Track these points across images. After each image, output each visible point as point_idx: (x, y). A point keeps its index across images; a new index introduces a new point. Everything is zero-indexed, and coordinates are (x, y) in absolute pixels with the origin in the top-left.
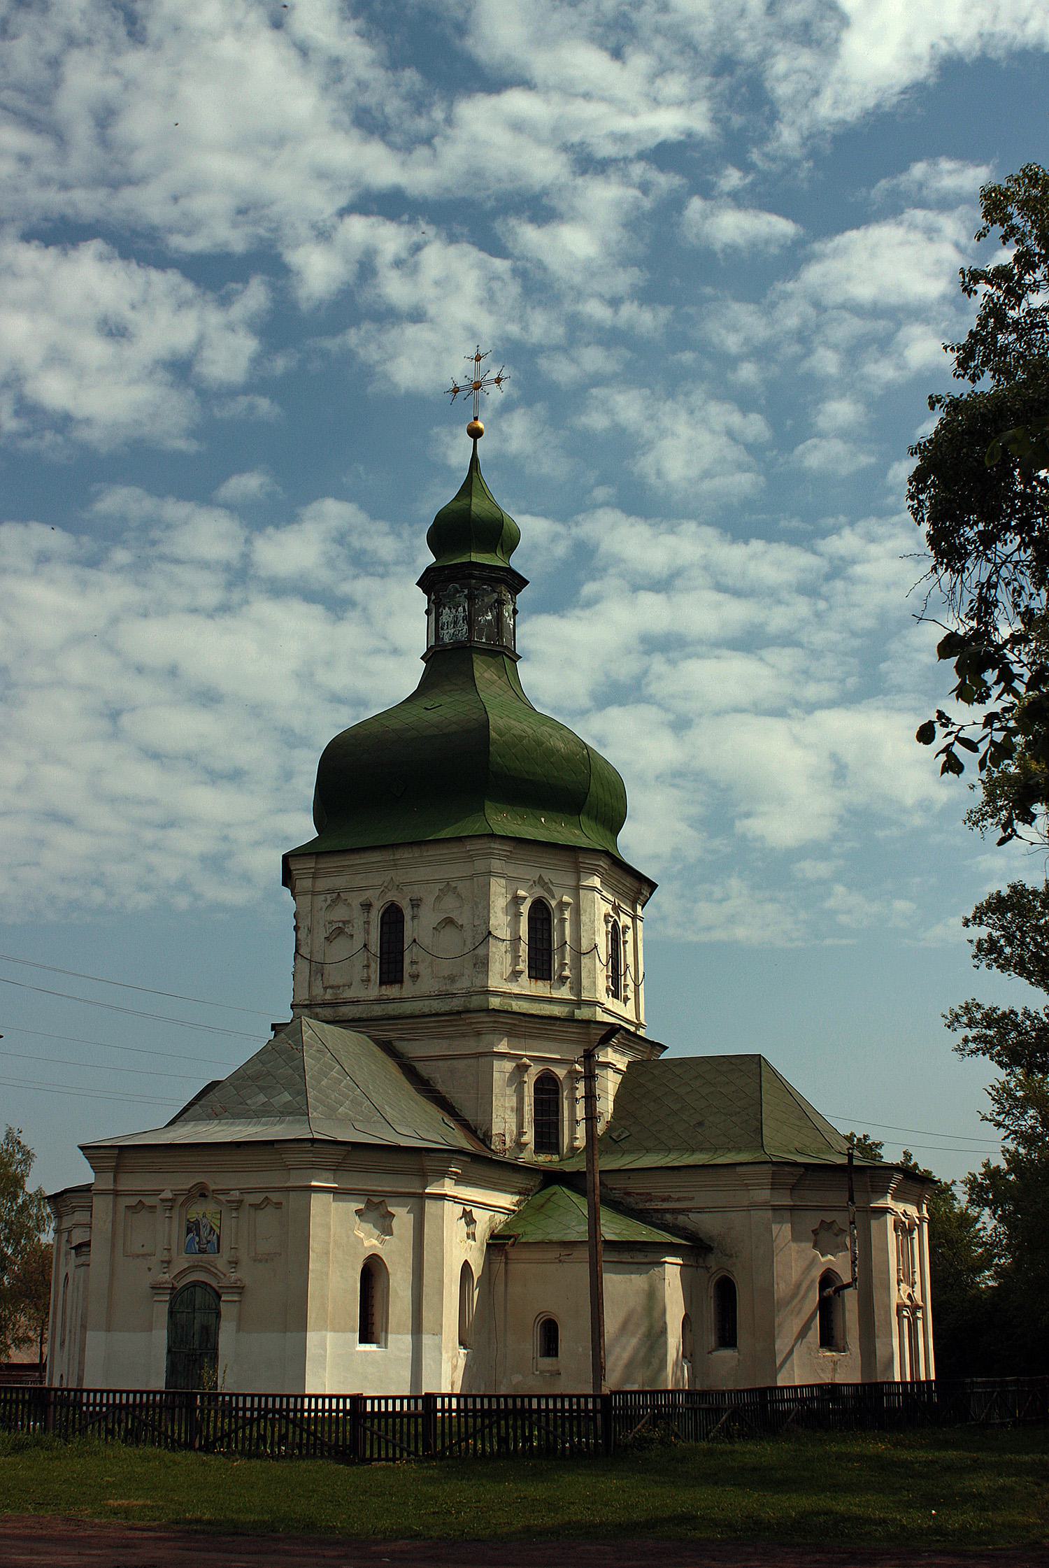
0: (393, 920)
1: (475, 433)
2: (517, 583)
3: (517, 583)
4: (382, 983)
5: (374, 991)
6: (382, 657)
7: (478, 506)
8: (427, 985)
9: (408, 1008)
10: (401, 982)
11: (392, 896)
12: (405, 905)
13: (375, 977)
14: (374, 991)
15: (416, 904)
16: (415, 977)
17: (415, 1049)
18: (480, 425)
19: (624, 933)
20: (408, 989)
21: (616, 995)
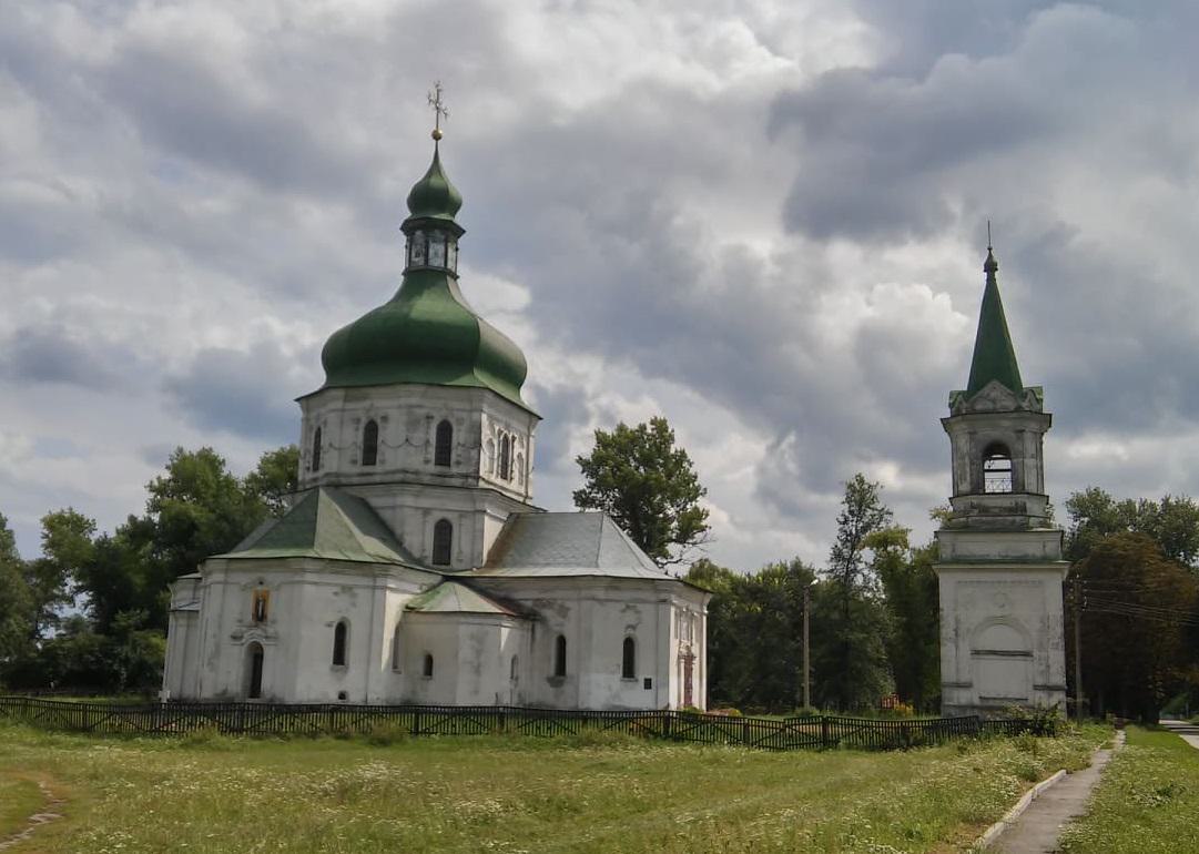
0: (372, 430)
1: (437, 137)
2: (459, 232)
3: (459, 232)
4: (366, 463)
5: (359, 468)
6: (373, 273)
7: (434, 181)
8: (388, 467)
9: (377, 479)
10: (374, 463)
11: (372, 414)
12: (379, 421)
13: (360, 462)
14: (359, 468)
15: (385, 419)
16: (383, 462)
17: (375, 502)
18: (441, 132)
19: (513, 441)
20: (378, 468)
21: (504, 476)
